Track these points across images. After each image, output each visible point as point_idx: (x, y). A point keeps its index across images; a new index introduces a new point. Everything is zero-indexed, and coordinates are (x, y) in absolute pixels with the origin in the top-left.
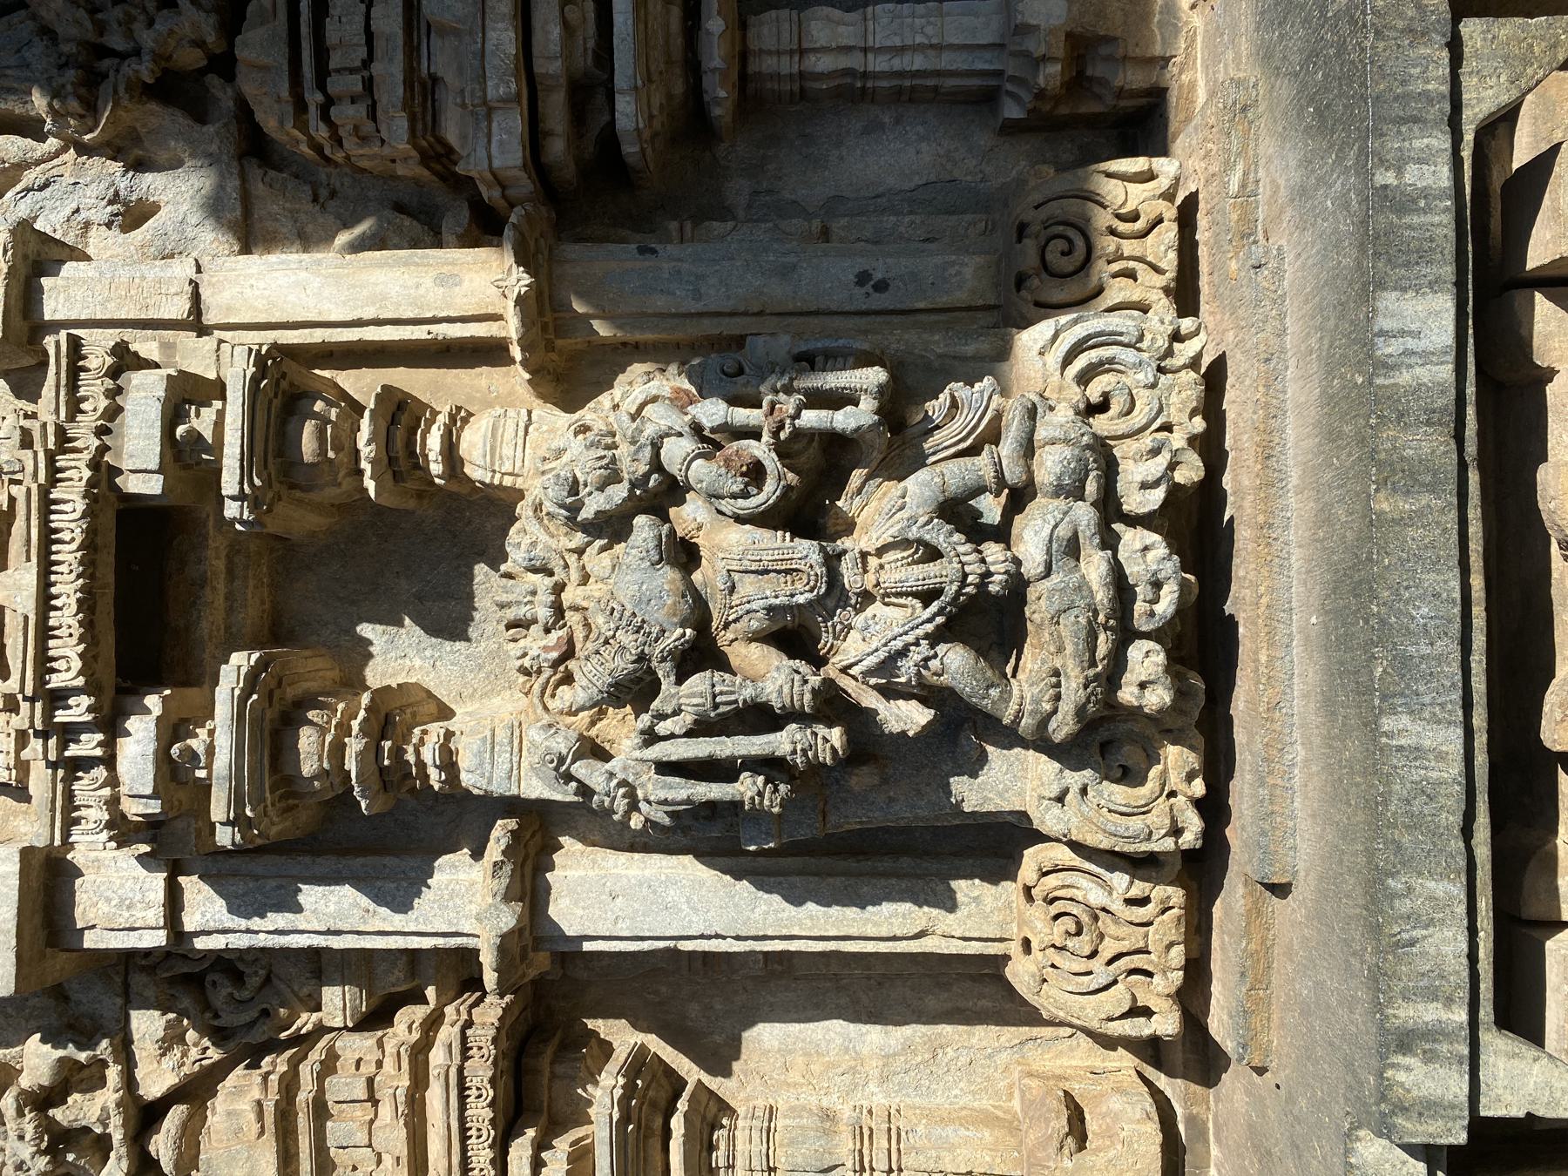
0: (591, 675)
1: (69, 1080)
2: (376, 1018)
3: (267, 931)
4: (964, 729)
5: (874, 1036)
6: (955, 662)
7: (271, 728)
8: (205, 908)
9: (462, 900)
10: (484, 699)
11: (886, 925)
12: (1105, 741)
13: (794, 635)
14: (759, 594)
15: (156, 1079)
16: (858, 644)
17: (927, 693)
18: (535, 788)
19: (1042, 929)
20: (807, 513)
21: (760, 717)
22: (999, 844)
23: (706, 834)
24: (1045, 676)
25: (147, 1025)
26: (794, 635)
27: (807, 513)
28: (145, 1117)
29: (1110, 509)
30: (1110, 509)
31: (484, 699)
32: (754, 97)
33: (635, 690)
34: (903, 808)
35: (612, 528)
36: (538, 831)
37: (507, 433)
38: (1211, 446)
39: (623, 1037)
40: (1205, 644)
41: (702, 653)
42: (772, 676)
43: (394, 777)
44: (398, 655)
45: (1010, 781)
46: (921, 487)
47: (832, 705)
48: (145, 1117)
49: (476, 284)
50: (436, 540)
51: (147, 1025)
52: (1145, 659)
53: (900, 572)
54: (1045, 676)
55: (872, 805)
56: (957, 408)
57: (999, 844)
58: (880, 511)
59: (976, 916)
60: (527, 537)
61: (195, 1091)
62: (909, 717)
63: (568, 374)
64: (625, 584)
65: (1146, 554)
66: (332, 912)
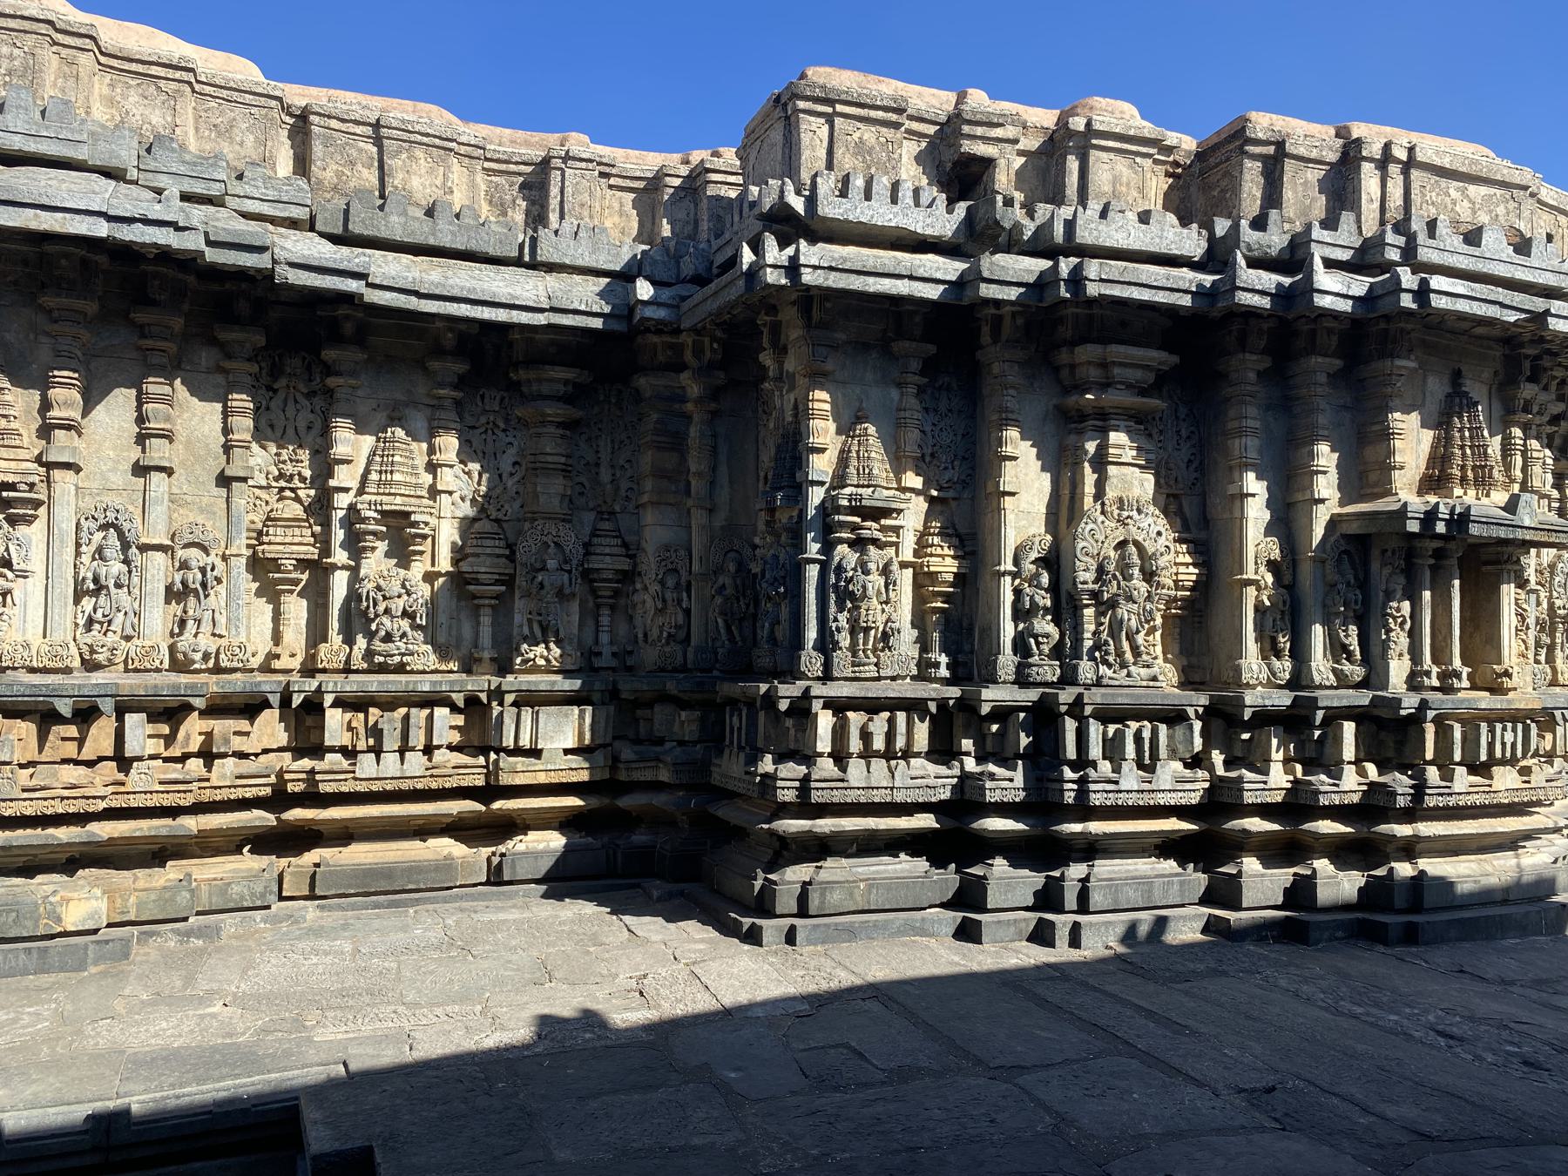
0: (381, 582)
1: (303, 479)
2: (313, 535)
3: (336, 524)
4: (370, 635)
5: (304, 622)
6: (383, 633)
7: (374, 533)
8: (341, 513)
9: (340, 556)
10: (376, 562)
11: (334, 624)
12: (369, 654)
13: (387, 611)
14: (393, 607)
15: (301, 493)
16: (386, 620)
17: (377, 631)
18: (363, 572)
19: (335, 648)
20: (405, 614)
21: (375, 604)
22: (349, 641)
23: (353, 596)
24: (378, 645)
25: (312, 492)
26: (387, 611)
27: (405, 614)
28: (293, 490)
29: (403, 655)
30: (403, 655)
31: (376, 562)
32: (478, 607)
33: (379, 588)
34: (357, 622)
35: (403, 586)
36: (354, 571)
37: (418, 568)
38: (412, 672)
39: (305, 577)
40: (383, 669)
41: (385, 598)
42: (381, 608)
43: (365, 549)
44: (382, 546)
45: (361, 643)
46: (408, 629)
47: (377, 616)
48: (293, 490)
49: (445, 565)
50: (402, 553)
51: (312, 492)
52: (382, 659)
53: (396, 626)
54: (378, 645)
56: (420, 636)
57: (349, 641)
58: (405, 624)
59: (336, 639)
60: (402, 572)
61: (298, 499)
62: (374, 627)
63: (429, 577)
64: (396, 588)
65: (397, 659)
66: (339, 535)
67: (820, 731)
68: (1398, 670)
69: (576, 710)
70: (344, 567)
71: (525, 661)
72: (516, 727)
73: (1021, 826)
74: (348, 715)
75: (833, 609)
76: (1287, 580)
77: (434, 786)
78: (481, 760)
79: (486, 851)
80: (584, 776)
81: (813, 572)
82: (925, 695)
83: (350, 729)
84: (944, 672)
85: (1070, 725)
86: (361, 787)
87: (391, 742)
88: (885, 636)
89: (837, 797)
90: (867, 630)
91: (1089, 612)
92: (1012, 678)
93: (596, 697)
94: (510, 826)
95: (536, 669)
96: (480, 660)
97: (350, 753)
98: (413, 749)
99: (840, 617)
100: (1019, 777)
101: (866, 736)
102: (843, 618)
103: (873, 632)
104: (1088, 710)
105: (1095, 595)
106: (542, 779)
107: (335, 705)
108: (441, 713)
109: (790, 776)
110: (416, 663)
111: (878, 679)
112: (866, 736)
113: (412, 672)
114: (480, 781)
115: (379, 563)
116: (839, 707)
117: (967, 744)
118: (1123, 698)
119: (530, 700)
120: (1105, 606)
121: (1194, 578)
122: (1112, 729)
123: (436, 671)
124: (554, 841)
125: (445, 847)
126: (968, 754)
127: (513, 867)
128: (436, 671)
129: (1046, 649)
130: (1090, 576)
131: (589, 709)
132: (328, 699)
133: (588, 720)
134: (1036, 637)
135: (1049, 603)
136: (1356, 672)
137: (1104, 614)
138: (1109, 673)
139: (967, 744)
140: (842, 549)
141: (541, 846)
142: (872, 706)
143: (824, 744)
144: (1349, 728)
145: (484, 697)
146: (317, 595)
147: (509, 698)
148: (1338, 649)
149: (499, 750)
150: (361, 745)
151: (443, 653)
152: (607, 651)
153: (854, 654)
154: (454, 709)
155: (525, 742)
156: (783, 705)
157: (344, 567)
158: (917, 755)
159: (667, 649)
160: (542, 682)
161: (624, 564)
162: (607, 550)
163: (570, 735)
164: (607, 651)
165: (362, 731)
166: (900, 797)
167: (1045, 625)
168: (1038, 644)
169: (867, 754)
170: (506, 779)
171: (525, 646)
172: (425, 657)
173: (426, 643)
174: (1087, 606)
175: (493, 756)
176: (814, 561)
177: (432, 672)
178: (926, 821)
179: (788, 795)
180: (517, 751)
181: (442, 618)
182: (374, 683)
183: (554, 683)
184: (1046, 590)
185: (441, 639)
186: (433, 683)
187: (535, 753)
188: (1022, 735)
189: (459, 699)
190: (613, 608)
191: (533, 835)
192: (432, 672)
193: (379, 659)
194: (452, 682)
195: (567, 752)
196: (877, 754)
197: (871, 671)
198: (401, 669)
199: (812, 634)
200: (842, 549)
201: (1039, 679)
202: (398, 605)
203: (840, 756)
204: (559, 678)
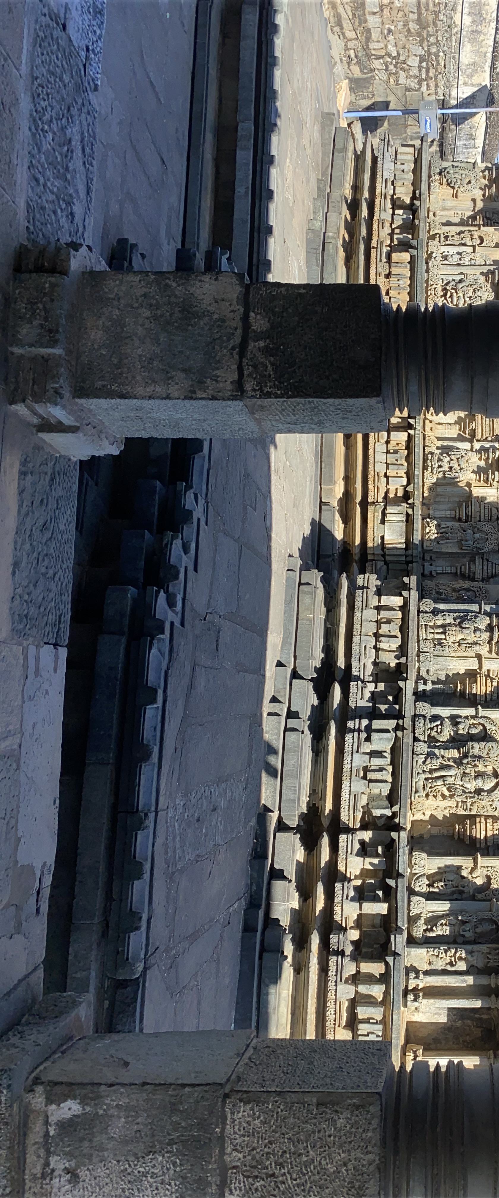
4: (441, 454)
11: (446, 443)
12: (432, 454)
13: (452, 460)
16: (448, 459)
22: (438, 448)
38: (423, 473)
40: (425, 460)
42: (453, 457)
45: (438, 452)
47: (449, 455)
55: (447, 451)
56: (441, 475)
65: (430, 464)
67: (392, 598)
68: (419, 957)
69: (403, 541)
70: (472, 446)
71: (428, 523)
72: (396, 515)
73: (335, 706)
74: (404, 443)
75: (456, 615)
76: (479, 896)
77: (370, 476)
78: (380, 500)
79: (335, 503)
80: (370, 544)
81: (475, 608)
82: (409, 654)
83: (398, 444)
84: (421, 687)
85: (390, 724)
86: (371, 446)
87: (391, 459)
88: (440, 644)
89: (358, 605)
90: (444, 633)
91: (455, 753)
92: (418, 713)
93: (409, 552)
94: (347, 518)
95: (424, 528)
96: (429, 509)
97: (388, 442)
98: (387, 468)
99: (451, 618)
100: (362, 703)
101: (389, 621)
102: (449, 620)
103: (443, 637)
104: (400, 734)
105: (466, 756)
106: (370, 525)
107: (409, 434)
108: (404, 481)
109: (370, 581)
110: (428, 473)
111: (418, 641)
112: (389, 621)
113: (423, 473)
114: (370, 500)
115: (475, 462)
116: (404, 608)
117: (381, 686)
118: (406, 756)
119: (409, 519)
120: (459, 762)
121: (478, 836)
122: (388, 755)
123: (423, 486)
124: (339, 534)
125: (339, 489)
126: (376, 687)
127: (328, 510)
128: (423, 486)
129: (433, 733)
130: (476, 751)
131: (404, 546)
132: (411, 432)
133: (398, 546)
134: (441, 724)
135: (461, 732)
136: (419, 932)
137: (454, 762)
138: (420, 761)
139: (381, 686)
140: (487, 620)
141: (336, 527)
142: (404, 628)
143: (386, 600)
144: (382, 908)
145: (411, 501)
146: (460, 438)
147: (410, 511)
148: (433, 921)
149: (385, 506)
150: (390, 447)
151: (430, 489)
152: (433, 568)
153: (432, 627)
154: (405, 487)
155: (389, 518)
156: (406, 580)
157: (472, 446)
158: (377, 656)
159: (434, 592)
160: (418, 524)
161: (479, 575)
162: (485, 567)
163: (391, 538)
164: (433, 568)
165: (397, 448)
166: (356, 639)
167: (447, 732)
168: (437, 726)
169: (379, 623)
170: (370, 509)
171: (436, 523)
172: (431, 479)
173: (437, 479)
174: (459, 753)
175: (382, 504)
176: (480, 608)
177: (423, 483)
178: (341, 663)
179: (360, 580)
180: (384, 514)
181: (449, 489)
182: (419, 450)
183: (417, 531)
184: (468, 733)
185: (439, 489)
186: (418, 476)
187: (383, 522)
188: (386, 706)
189: (410, 488)
190: (456, 573)
191: (342, 526)
192: (423, 483)
193: (430, 457)
194: (418, 483)
195: (383, 538)
196: (379, 627)
197: (423, 636)
198: (425, 468)
199: (442, 606)
200: (487, 620)
201: (417, 723)
202: (455, 465)
203: (378, 608)
204: (420, 538)
